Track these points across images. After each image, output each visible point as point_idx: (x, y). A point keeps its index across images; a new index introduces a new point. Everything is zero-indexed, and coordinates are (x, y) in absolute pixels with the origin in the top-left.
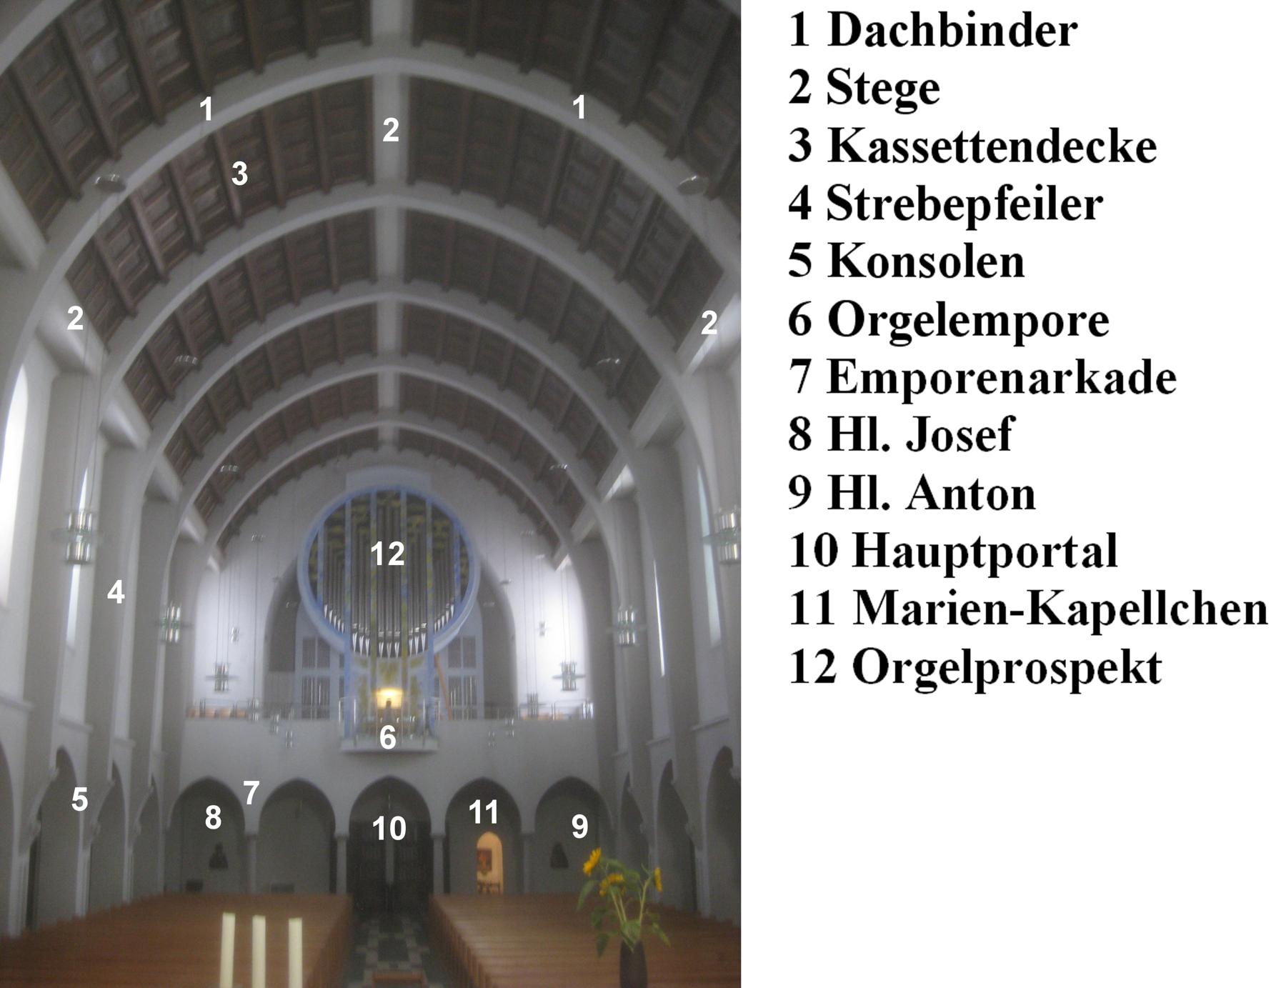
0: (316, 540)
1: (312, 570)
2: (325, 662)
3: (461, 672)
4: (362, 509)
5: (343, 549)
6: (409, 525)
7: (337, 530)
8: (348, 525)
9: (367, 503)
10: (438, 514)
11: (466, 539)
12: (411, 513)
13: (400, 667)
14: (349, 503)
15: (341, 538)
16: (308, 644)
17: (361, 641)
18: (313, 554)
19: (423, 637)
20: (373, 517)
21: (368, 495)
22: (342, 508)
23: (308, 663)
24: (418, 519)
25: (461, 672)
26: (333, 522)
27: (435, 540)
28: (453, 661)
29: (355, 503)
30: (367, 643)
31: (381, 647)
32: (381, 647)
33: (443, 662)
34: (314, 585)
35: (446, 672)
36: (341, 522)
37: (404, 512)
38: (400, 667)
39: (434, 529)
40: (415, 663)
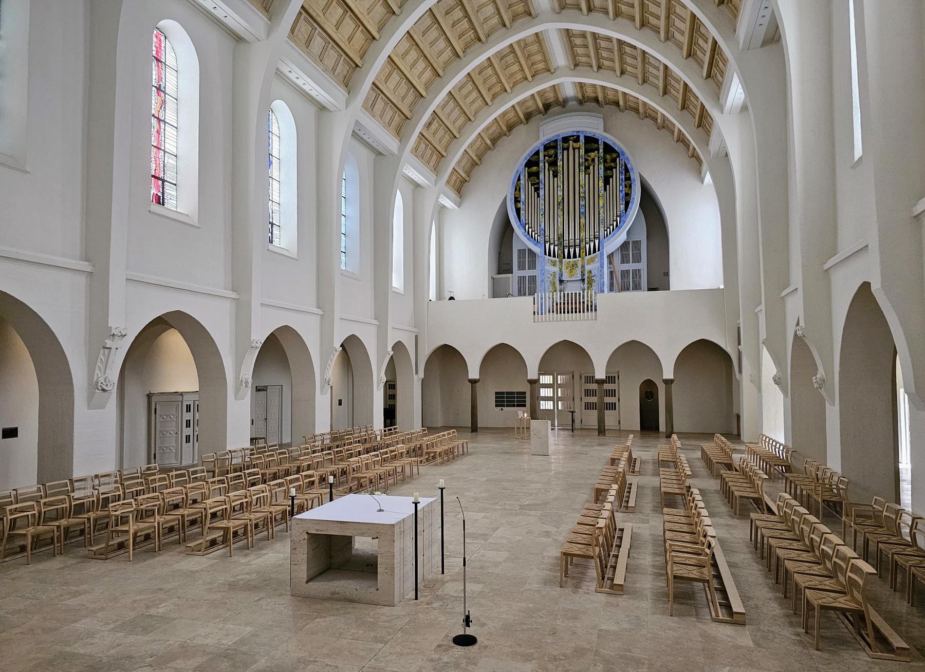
0: (519, 179)
1: (517, 200)
2: (533, 266)
3: (631, 266)
4: (552, 152)
5: (538, 183)
6: (586, 160)
7: (535, 168)
8: (541, 165)
9: (555, 147)
10: (608, 149)
11: (629, 166)
12: (587, 151)
13: (580, 264)
14: (542, 149)
15: (537, 174)
16: (521, 252)
17: (552, 247)
18: (517, 189)
19: (597, 242)
20: (560, 157)
21: (556, 140)
22: (537, 153)
23: (521, 267)
24: (592, 154)
25: (631, 266)
26: (532, 163)
27: (606, 169)
28: (624, 260)
29: (546, 147)
30: (556, 248)
31: (566, 251)
32: (566, 251)
33: (617, 259)
34: (518, 211)
35: (619, 267)
36: (537, 164)
37: (582, 152)
38: (580, 264)
39: (605, 161)
40: (592, 260)
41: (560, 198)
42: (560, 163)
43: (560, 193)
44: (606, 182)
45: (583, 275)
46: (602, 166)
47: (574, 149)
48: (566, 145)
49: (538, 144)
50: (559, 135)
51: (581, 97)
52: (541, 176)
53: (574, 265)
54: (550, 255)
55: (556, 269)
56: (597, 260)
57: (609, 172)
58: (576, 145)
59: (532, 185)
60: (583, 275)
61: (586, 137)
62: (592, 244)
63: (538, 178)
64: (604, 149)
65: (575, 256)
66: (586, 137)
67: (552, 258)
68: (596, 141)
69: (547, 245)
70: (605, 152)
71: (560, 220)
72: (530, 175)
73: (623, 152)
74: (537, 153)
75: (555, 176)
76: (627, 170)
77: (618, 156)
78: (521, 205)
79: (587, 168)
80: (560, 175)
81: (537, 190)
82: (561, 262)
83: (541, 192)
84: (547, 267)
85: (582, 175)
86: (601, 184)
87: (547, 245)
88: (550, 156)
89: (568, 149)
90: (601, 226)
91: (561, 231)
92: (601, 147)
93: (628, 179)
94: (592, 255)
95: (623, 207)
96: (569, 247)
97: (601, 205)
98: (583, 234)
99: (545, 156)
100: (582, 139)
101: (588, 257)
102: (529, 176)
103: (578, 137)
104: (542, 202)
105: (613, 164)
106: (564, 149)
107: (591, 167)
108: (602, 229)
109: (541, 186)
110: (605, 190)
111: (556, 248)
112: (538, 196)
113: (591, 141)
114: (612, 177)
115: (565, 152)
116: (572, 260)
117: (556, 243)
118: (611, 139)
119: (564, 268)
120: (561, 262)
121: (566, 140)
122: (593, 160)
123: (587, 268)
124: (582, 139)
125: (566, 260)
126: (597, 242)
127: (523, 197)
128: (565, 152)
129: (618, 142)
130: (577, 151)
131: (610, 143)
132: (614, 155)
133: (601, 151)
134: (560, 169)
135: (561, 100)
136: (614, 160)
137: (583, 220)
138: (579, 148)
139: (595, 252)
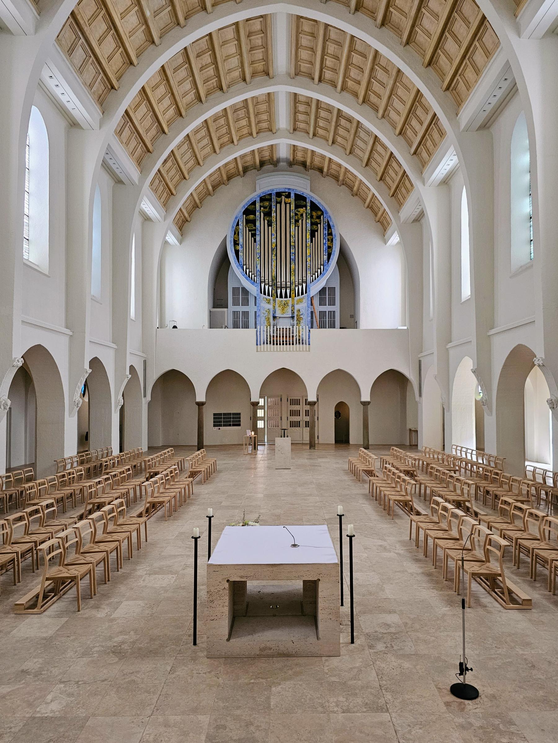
0: (238, 225)
1: (236, 243)
4: (267, 204)
5: (255, 230)
6: (296, 214)
7: (252, 217)
8: (258, 214)
9: (270, 200)
11: (331, 223)
12: (297, 207)
13: (290, 304)
14: (258, 200)
15: (254, 222)
18: (236, 233)
19: (304, 285)
20: (274, 209)
21: (271, 194)
22: (254, 203)
24: (302, 210)
26: (249, 211)
27: (312, 224)
29: (262, 199)
30: (270, 288)
34: (237, 252)
38: (290, 304)
39: (312, 217)
40: (300, 301)
41: (274, 245)
42: (273, 214)
43: (274, 241)
44: (313, 235)
45: (293, 313)
46: (309, 221)
47: (286, 204)
48: (279, 199)
49: (254, 196)
50: (273, 190)
51: (292, 160)
52: (258, 224)
53: (286, 304)
54: (265, 294)
55: (271, 307)
56: (304, 301)
57: (315, 227)
58: (287, 200)
59: (249, 231)
60: (293, 313)
61: (296, 195)
62: (300, 287)
63: (255, 226)
64: (311, 207)
65: (286, 297)
66: (296, 195)
67: (266, 296)
68: (304, 199)
69: (263, 285)
70: (312, 210)
71: (274, 264)
72: (248, 222)
73: (326, 211)
74: (254, 203)
75: (270, 225)
76: (329, 227)
77: (323, 214)
78: (239, 248)
79: (297, 221)
80: (274, 225)
81: (254, 235)
82: (274, 300)
83: (258, 238)
84: (262, 305)
85: (293, 227)
86: (309, 236)
87: (263, 285)
88: (265, 208)
89: (280, 203)
90: (308, 272)
91: (274, 274)
92: (309, 204)
93: (330, 234)
94: (301, 296)
95: (326, 257)
96: (281, 288)
97: (308, 254)
98: (293, 278)
99: (261, 207)
100: (292, 195)
101: (297, 298)
102: (246, 223)
103: (290, 193)
104: (258, 247)
105: (318, 220)
106: (277, 203)
107: (300, 221)
108: (309, 275)
109: (258, 233)
110: (312, 241)
111: (270, 288)
112: (255, 241)
113: (300, 199)
114: (317, 231)
115: (278, 205)
116: (284, 299)
117: (270, 283)
118: (317, 200)
119: (277, 306)
120: (274, 300)
121: (279, 194)
122: (302, 215)
123: (297, 307)
124: (292, 195)
125: (279, 299)
126: (304, 285)
127: (241, 240)
128: (278, 205)
129: (323, 203)
130: (288, 205)
131: (314, 202)
132: (319, 213)
133: (308, 208)
134: (274, 219)
135: (275, 159)
136: (319, 217)
137: (293, 266)
138: (290, 203)
139: (302, 294)
